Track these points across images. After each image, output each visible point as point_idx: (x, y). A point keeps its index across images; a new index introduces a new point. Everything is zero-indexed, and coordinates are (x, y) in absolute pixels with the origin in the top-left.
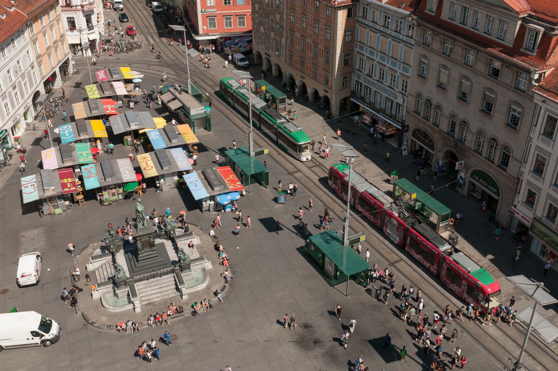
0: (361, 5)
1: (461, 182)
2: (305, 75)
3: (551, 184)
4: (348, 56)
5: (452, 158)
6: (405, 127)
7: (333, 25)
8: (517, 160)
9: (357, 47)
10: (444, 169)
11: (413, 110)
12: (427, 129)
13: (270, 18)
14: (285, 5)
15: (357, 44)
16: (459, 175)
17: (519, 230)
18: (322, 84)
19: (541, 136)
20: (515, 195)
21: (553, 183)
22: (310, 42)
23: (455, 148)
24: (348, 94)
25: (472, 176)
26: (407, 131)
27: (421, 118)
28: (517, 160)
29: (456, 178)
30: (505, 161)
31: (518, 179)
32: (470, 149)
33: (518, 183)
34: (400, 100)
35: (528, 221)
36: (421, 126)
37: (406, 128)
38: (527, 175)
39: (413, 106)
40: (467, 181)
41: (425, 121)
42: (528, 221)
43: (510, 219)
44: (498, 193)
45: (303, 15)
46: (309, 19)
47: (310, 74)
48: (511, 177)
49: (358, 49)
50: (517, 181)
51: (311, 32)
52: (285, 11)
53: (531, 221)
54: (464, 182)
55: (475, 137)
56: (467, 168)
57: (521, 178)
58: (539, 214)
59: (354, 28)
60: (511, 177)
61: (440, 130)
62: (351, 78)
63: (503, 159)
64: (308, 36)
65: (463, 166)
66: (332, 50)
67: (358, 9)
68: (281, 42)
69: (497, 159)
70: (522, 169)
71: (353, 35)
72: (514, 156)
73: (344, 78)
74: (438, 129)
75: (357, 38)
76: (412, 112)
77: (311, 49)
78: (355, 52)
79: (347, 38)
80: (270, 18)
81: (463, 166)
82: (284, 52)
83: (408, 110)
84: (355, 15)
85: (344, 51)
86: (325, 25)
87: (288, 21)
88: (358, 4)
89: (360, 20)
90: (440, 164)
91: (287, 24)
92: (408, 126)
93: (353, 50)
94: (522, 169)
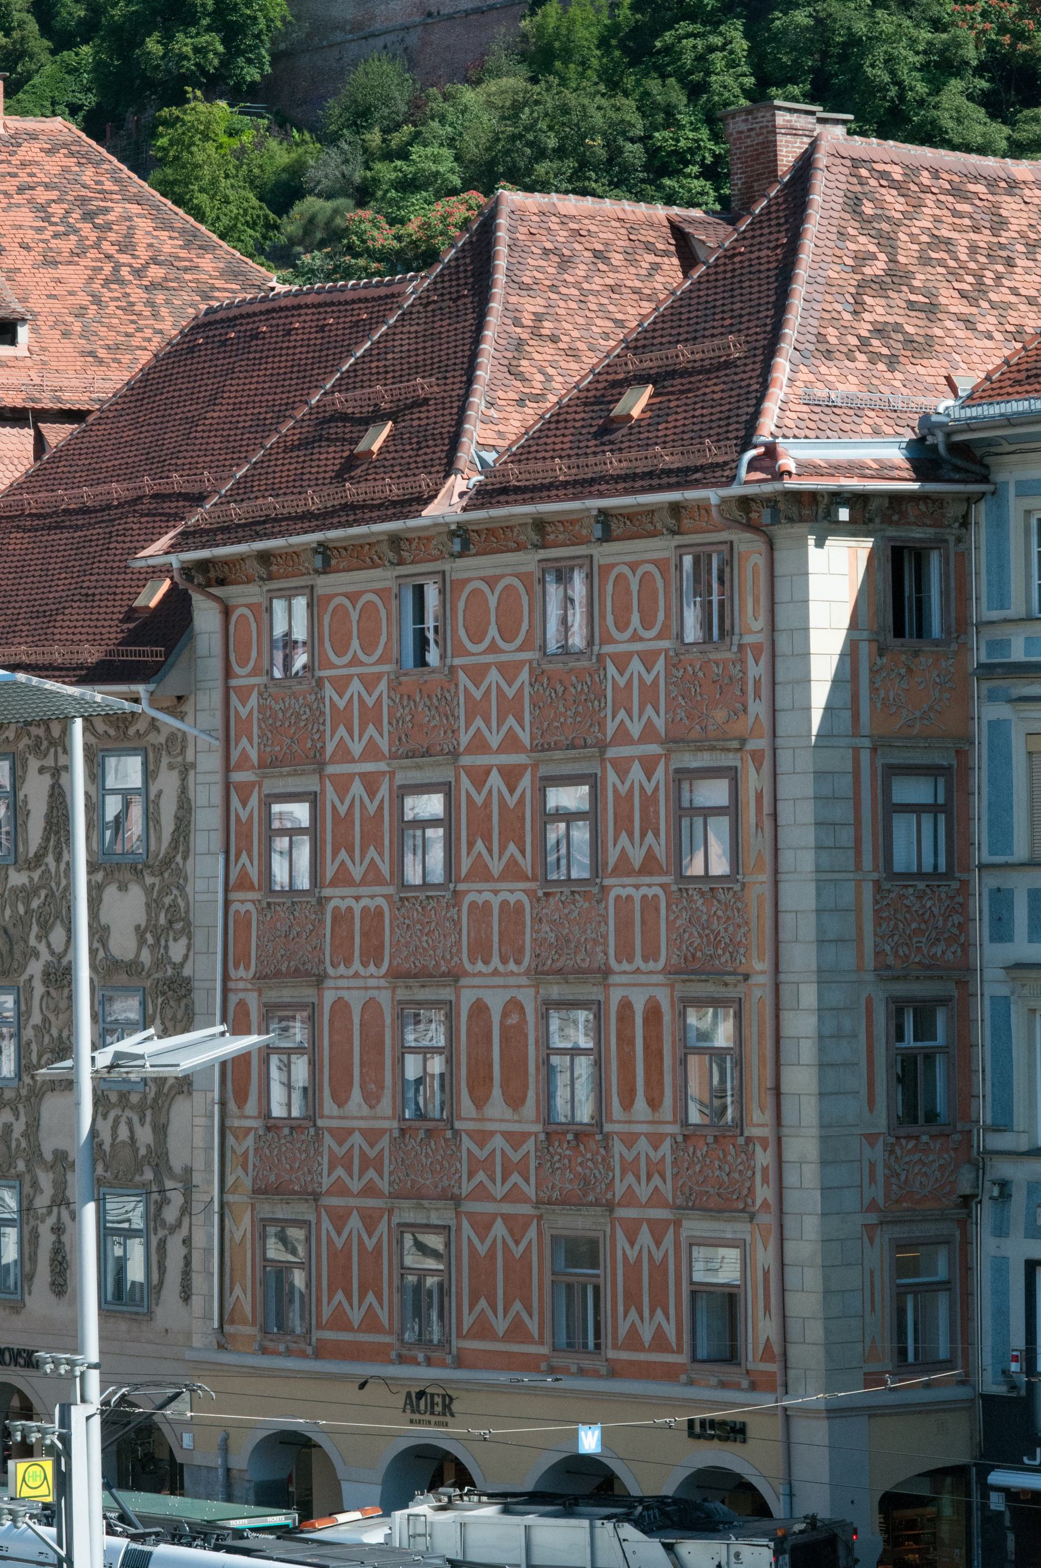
0: (1015, 506)
2: (459, 1363)
4: (924, 1030)
7: (758, 709)
9: (1002, 932)
13: (35, 968)
14: (208, 762)
15: (1001, 898)
18: (669, 1374)
22: (496, 1002)
24: (953, 1445)
45: (266, 1210)
46: (480, 776)
47: (517, 1331)
49: (1024, 948)
51: (515, 893)
52: (207, 820)
59: (962, 746)
62: (965, 1268)
64: (481, 950)
66: (761, 966)
67: (980, 560)
68: (159, 1158)
71: (950, 811)
73: (902, 1268)
75: (1002, 836)
77: (515, 1067)
78: (991, 985)
79: (903, 828)
80: (35, 968)
82: (206, 1234)
84: (960, 626)
85: (884, 972)
86: (674, 741)
87: (245, 903)
88: (981, 512)
89: (1018, 654)
91: (234, 927)
93: (963, 974)
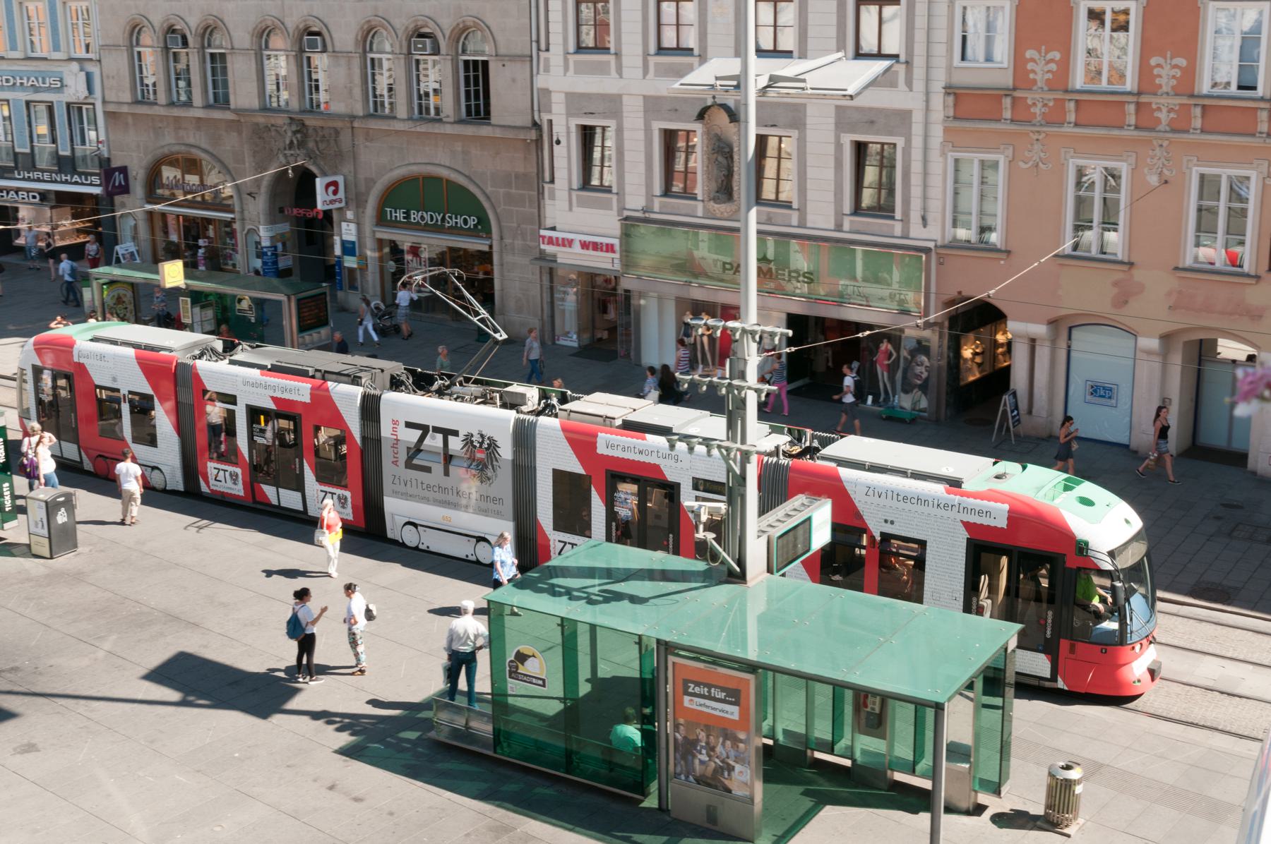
1: (350, 262)
3: (646, 54)
5: (300, 187)
6: (114, 177)
8: (514, 58)
10: (283, 263)
11: (127, 97)
12: (191, 141)
16: (337, 239)
17: (586, 337)
19: (574, 194)
20: (541, 193)
21: (652, 48)
23: (302, 144)
25: (381, 220)
26: (125, 189)
27: (162, 111)
28: (514, 58)
29: (326, 247)
30: (476, 77)
31: (536, 126)
32: (353, 117)
33: (539, 142)
34: (76, 89)
35: (610, 248)
36: (169, 141)
37: (118, 178)
38: (562, 78)
39: (127, 83)
40: (369, 243)
41: (176, 112)
42: (610, 248)
43: (546, 278)
44: (483, 229)
48: (510, 134)
50: (533, 135)
53: (616, 242)
54: (363, 258)
55: (356, 63)
56: (356, 199)
57: (545, 117)
58: (635, 202)
60: (510, 134)
61: (236, 111)
63: (468, 93)
65: (341, 194)
69: (448, 103)
70: (540, 82)
72: (502, 51)
74: (228, 116)
76: (125, 109)
81: (341, 194)
83: (111, 108)
90: (266, 243)
92: (124, 170)
94: (540, 82)
